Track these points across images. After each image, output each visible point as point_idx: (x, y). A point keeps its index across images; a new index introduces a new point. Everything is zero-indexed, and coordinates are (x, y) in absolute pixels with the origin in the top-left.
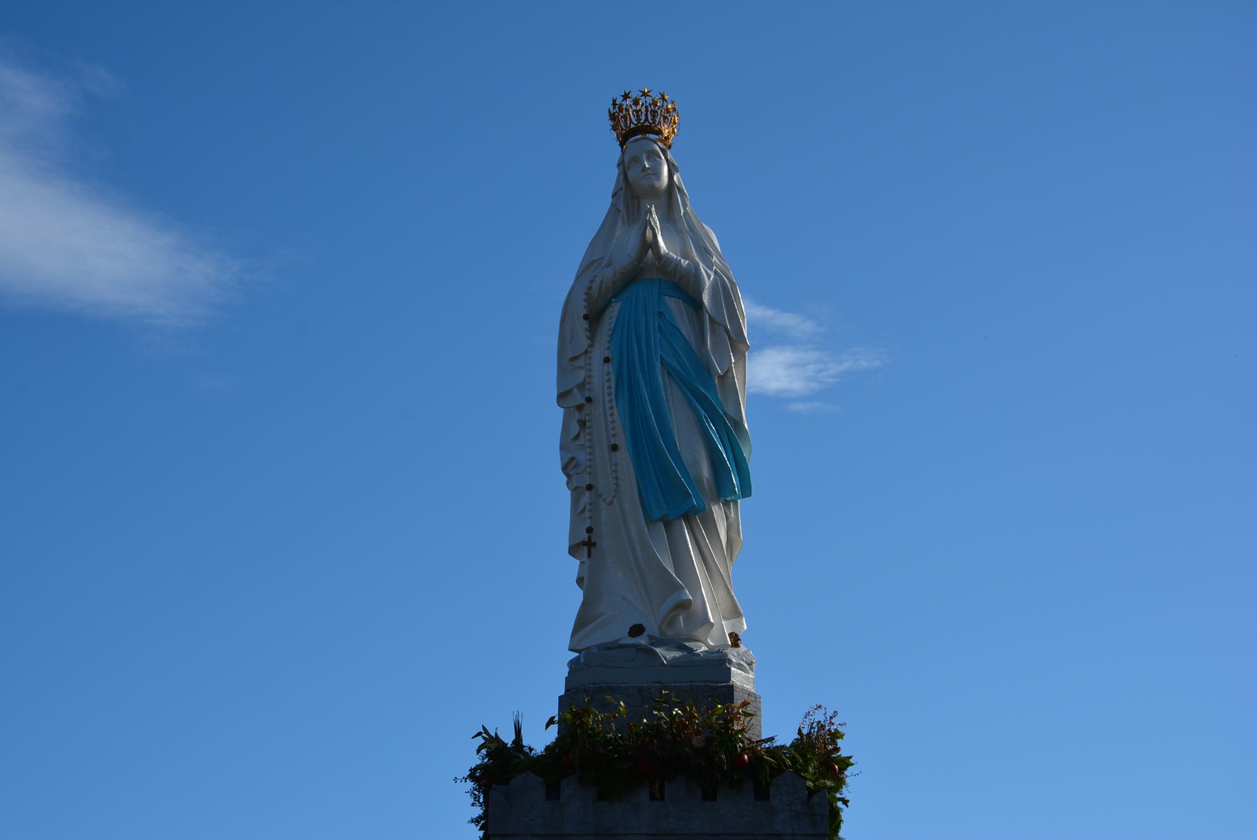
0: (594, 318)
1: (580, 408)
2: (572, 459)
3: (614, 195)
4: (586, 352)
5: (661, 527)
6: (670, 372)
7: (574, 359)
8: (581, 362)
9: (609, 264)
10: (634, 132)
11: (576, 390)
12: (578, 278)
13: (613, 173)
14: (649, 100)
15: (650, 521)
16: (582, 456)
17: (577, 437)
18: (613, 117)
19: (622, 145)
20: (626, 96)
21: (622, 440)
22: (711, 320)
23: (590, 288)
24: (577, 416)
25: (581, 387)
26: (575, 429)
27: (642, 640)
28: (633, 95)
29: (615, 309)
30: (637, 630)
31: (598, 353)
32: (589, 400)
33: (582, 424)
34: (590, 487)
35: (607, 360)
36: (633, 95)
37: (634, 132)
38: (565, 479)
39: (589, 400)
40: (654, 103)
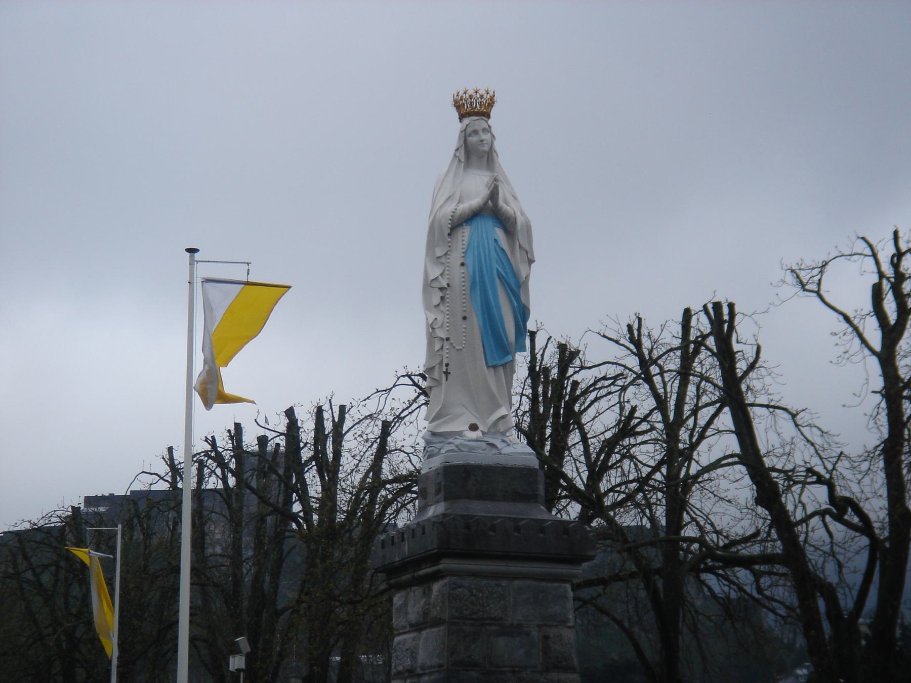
1: (441, 289)
3: (457, 150)
4: (446, 254)
8: (443, 260)
15: (488, 367)
17: (438, 305)
22: (520, 246)
25: (442, 275)
29: (465, 233)
31: (456, 257)
33: (442, 298)
35: (463, 264)
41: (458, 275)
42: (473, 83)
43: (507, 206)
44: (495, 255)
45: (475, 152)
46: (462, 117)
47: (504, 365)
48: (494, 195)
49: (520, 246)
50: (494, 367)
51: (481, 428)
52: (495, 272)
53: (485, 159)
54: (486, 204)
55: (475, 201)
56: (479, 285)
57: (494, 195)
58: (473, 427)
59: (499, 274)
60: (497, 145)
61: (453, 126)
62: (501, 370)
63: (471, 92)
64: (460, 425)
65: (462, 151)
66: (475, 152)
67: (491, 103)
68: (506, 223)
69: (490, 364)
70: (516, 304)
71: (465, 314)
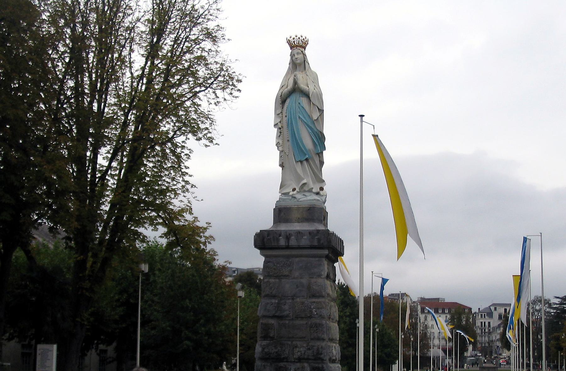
1: (280, 128)
5: (300, 163)
6: (302, 120)
8: (280, 115)
13: (289, 58)
15: (297, 162)
16: (281, 142)
21: (290, 139)
25: (280, 122)
27: (295, 192)
29: (288, 101)
33: (281, 132)
40: (299, 38)
42: (297, 31)
43: (303, 86)
44: (298, 110)
45: (298, 63)
46: (291, 49)
48: (295, 82)
50: (301, 162)
51: (297, 190)
52: (298, 118)
56: (290, 124)
57: (295, 82)
59: (299, 117)
62: (305, 163)
63: (299, 36)
64: (289, 190)
66: (298, 63)
68: (306, 95)
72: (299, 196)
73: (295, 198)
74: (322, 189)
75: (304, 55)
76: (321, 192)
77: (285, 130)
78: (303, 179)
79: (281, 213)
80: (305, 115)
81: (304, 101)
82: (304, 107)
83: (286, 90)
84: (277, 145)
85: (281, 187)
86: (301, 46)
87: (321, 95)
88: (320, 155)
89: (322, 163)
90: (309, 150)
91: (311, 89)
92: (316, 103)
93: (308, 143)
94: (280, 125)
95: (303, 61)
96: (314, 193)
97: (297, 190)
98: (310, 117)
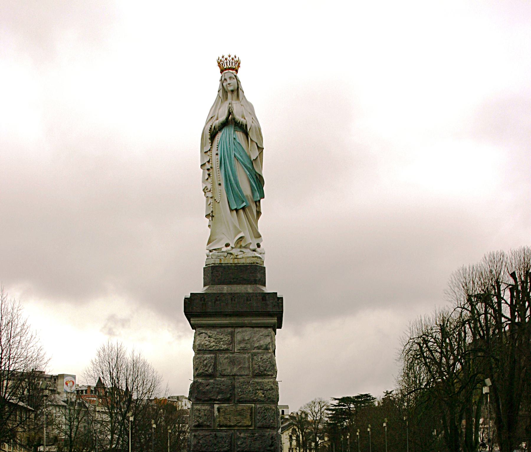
0: (213, 137)
1: (208, 170)
2: (206, 187)
3: (219, 91)
4: (210, 150)
5: (235, 212)
7: (206, 152)
9: (217, 119)
10: (226, 69)
11: (207, 163)
12: (207, 124)
14: (231, 58)
15: (231, 210)
16: (209, 187)
17: (208, 179)
18: (219, 63)
19: (221, 72)
20: (223, 57)
22: (251, 139)
23: (211, 128)
24: (207, 172)
25: (209, 162)
26: (207, 176)
27: (229, 248)
28: (225, 57)
30: (227, 245)
32: (212, 168)
33: (209, 175)
34: (212, 198)
35: (217, 154)
36: (225, 57)
37: (226, 69)
38: (204, 193)
39: (212, 168)
41: (215, 160)
42: (228, 51)
43: (239, 118)
45: (230, 90)
47: (243, 208)
49: (251, 139)
50: (237, 210)
51: (232, 245)
52: (233, 156)
53: (235, 93)
54: (227, 118)
55: (222, 118)
57: (230, 113)
58: (227, 245)
60: (244, 85)
61: (215, 76)
62: (241, 212)
64: (221, 245)
65: (221, 91)
66: (230, 90)
67: (238, 63)
68: (243, 128)
69: (233, 208)
70: (248, 173)
71: (219, 182)
72: (235, 252)
73: (231, 254)
74: (259, 246)
75: (238, 81)
76: (258, 249)
77: (214, 172)
78: (240, 232)
79: (215, 273)
80: (242, 154)
81: (240, 136)
82: (241, 143)
83: (217, 123)
84: (204, 190)
85: (209, 242)
86: (233, 69)
87: (260, 130)
88: (257, 203)
89: (259, 213)
90: (247, 196)
91: (248, 121)
92: (255, 139)
93: (246, 189)
94: (208, 166)
95: (236, 88)
96: (251, 250)
97: (232, 245)
98: (249, 158)
